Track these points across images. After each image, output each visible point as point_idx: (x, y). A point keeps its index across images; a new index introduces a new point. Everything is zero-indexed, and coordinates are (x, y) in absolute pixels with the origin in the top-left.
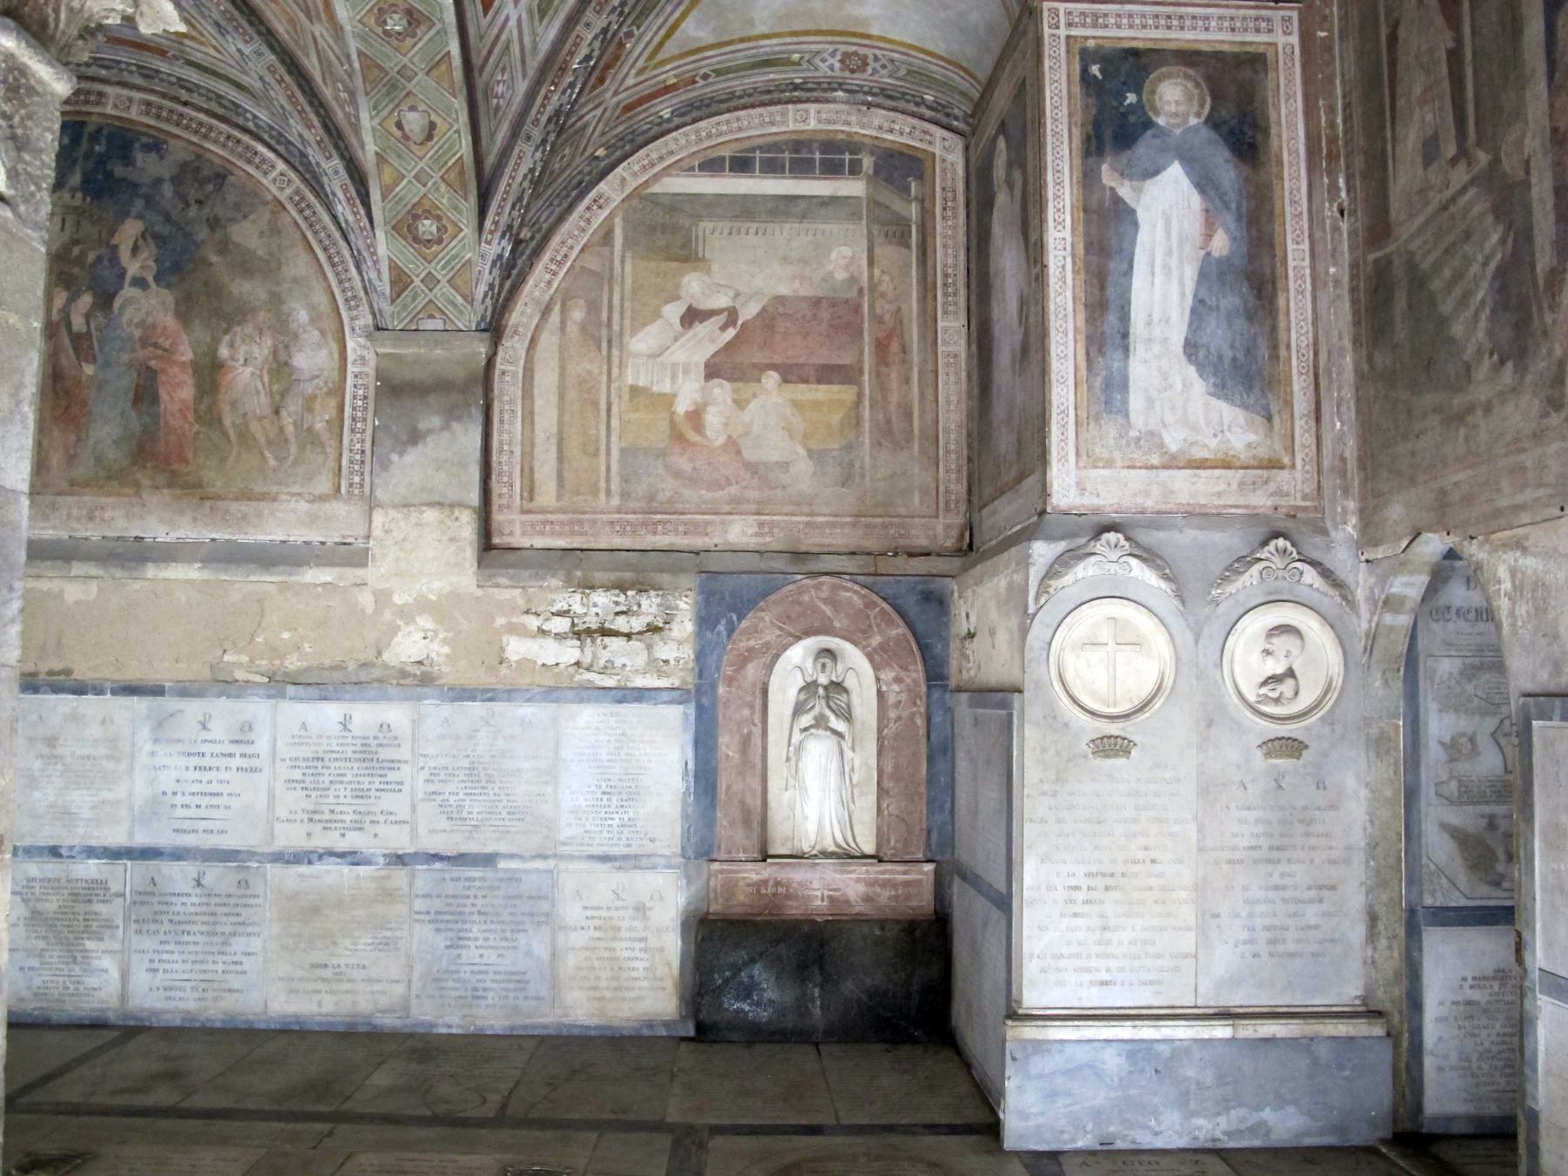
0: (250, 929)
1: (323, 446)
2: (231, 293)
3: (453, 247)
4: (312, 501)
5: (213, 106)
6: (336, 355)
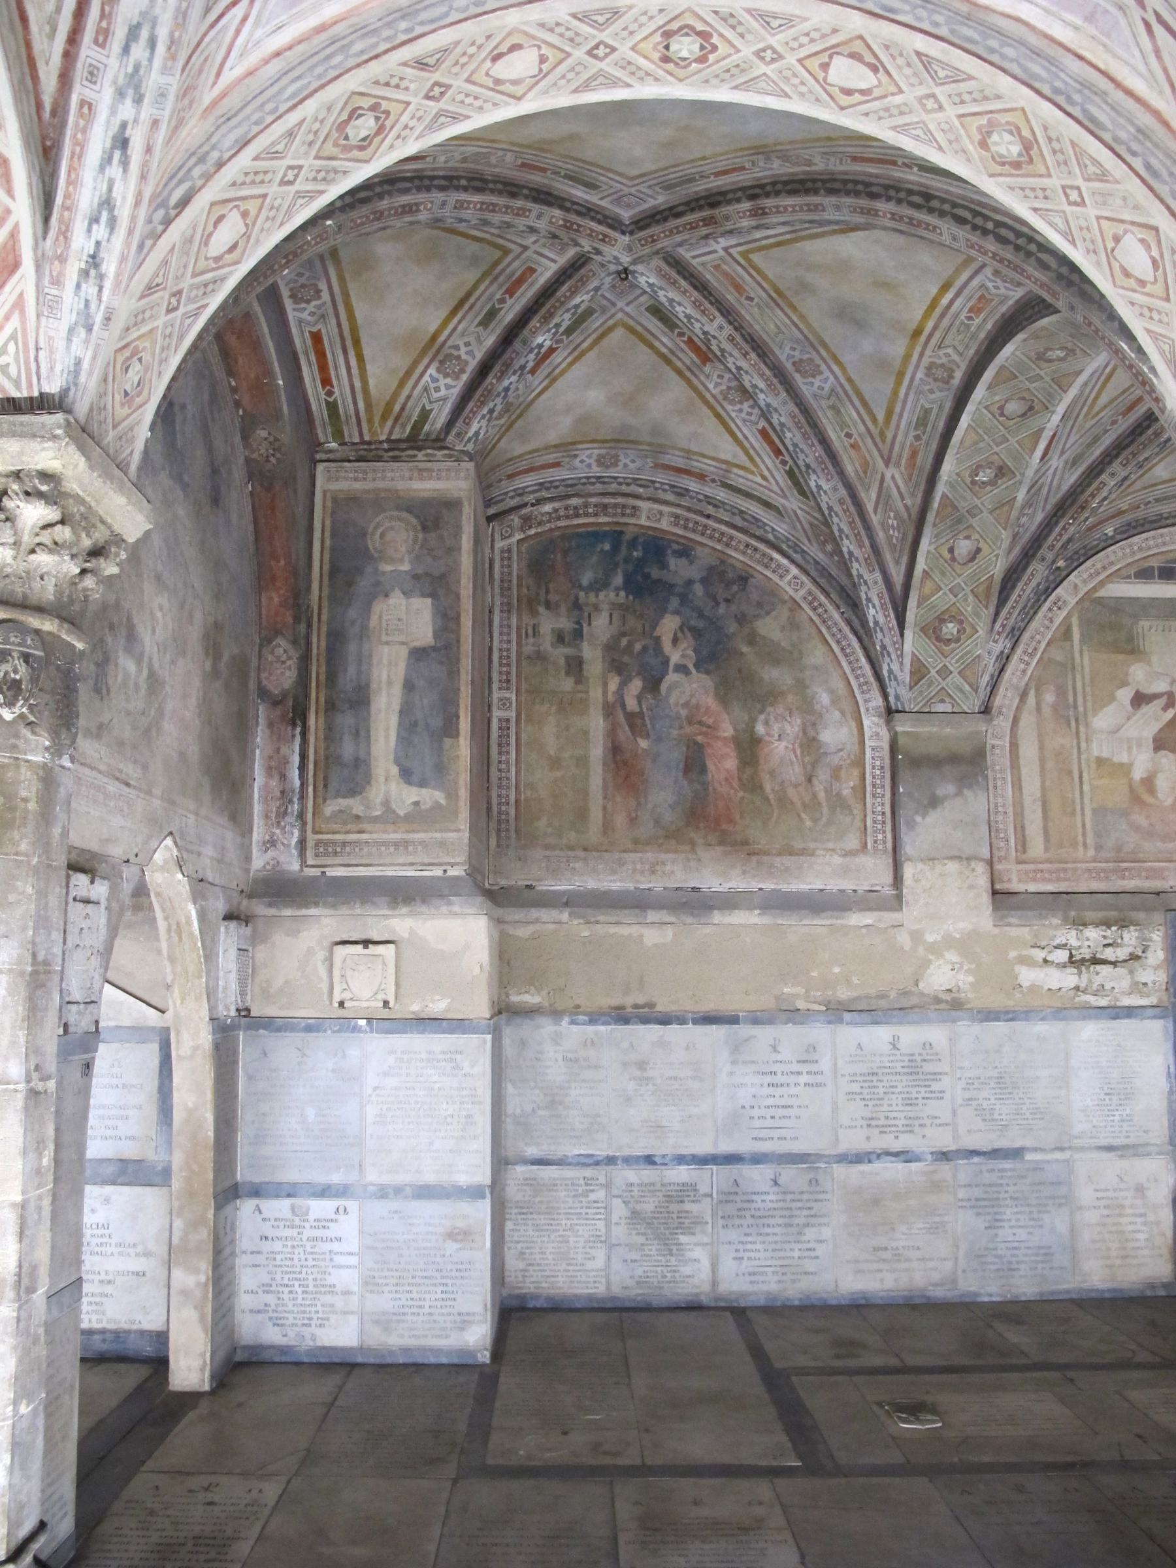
0: (822, 1220)
1: (849, 808)
2: (761, 680)
3: (968, 645)
4: (845, 855)
5: (738, 521)
6: (855, 732)
